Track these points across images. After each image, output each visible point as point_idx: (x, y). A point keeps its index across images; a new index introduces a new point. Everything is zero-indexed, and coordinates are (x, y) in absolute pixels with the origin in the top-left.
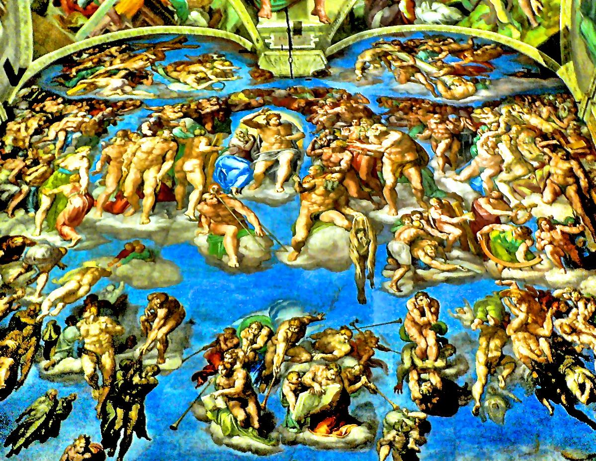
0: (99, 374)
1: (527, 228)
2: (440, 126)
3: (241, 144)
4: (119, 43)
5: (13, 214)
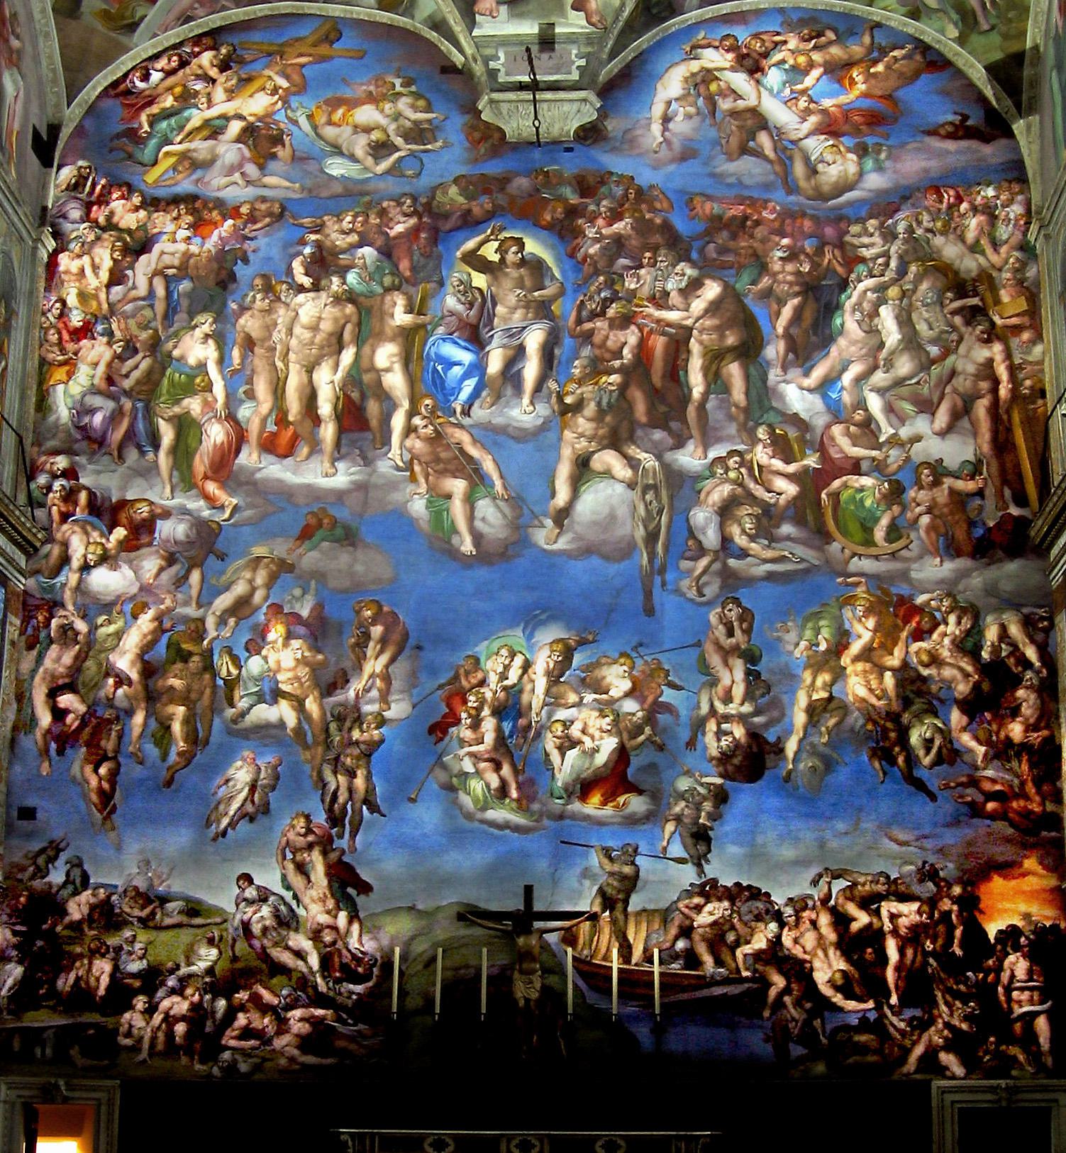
0: (307, 727)
1: (898, 482)
2: (790, 267)
3: (460, 308)
4: (212, 38)
5: (120, 457)
